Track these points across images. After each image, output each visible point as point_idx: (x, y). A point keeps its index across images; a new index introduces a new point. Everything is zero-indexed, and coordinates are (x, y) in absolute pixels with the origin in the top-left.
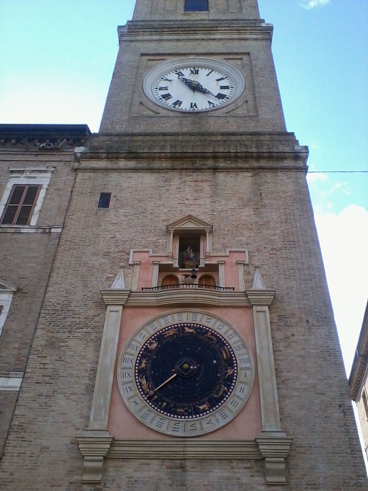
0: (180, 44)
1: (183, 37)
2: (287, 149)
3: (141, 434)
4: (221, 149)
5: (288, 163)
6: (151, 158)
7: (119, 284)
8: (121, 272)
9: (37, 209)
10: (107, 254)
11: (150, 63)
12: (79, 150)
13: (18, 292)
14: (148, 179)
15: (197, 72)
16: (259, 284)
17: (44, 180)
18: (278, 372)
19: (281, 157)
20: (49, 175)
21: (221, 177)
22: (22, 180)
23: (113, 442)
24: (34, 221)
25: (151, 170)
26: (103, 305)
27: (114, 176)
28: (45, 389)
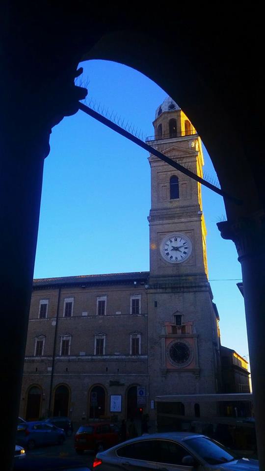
0: (170, 225)
1: (171, 221)
2: (203, 284)
3: (172, 368)
4: (185, 285)
5: (204, 289)
6: (166, 288)
7: (163, 333)
8: (163, 328)
9: (140, 308)
10: (159, 322)
11: (162, 236)
12: (146, 286)
13: (141, 334)
14: (165, 296)
15: (176, 240)
16: (195, 332)
17: (139, 297)
18: (198, 353)
19: (201, 287)
20: (140, 295)
21: (185, 294)
22: (134, 298)
23: (167, 369)
24: (140, 313)
25: (166, 293)
26: (160, 338)
27: (157, 295)
28: (152, 358)
